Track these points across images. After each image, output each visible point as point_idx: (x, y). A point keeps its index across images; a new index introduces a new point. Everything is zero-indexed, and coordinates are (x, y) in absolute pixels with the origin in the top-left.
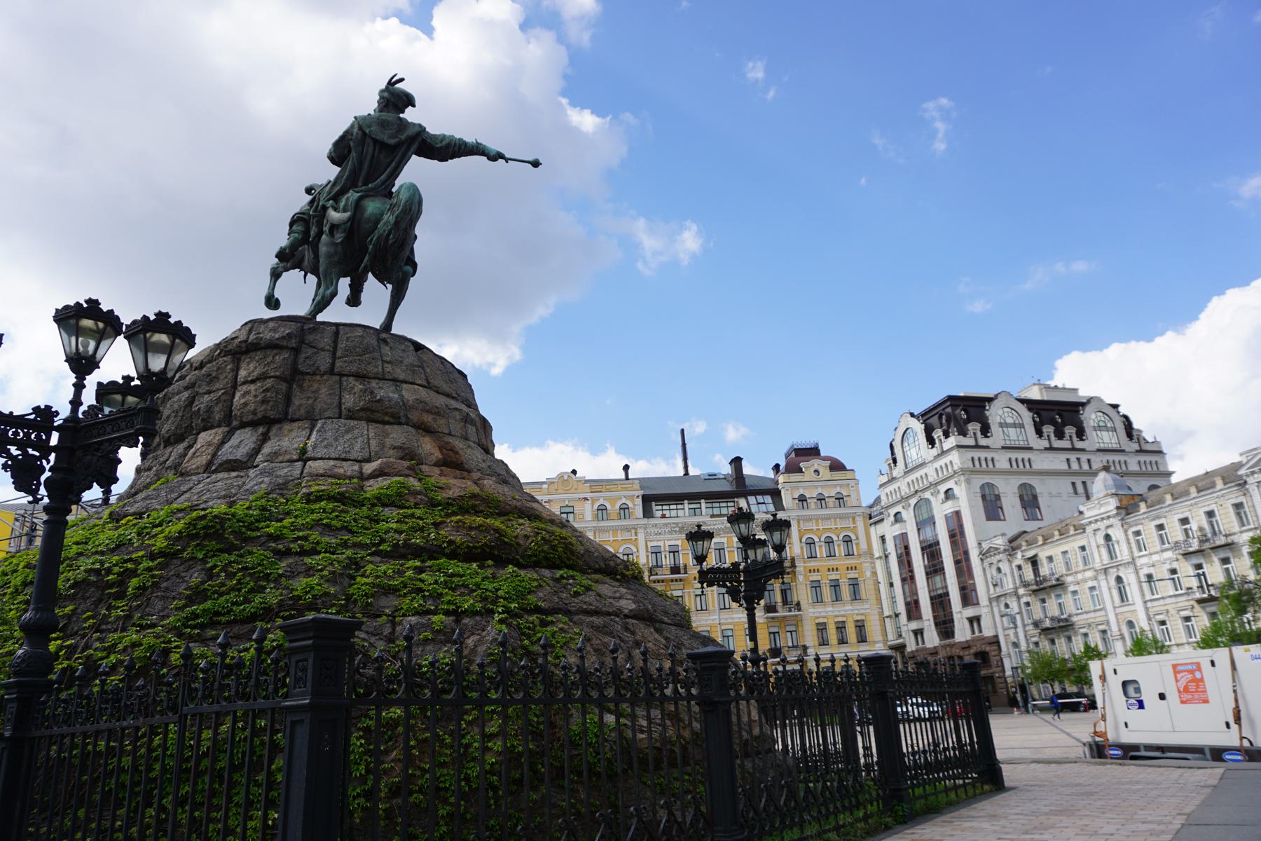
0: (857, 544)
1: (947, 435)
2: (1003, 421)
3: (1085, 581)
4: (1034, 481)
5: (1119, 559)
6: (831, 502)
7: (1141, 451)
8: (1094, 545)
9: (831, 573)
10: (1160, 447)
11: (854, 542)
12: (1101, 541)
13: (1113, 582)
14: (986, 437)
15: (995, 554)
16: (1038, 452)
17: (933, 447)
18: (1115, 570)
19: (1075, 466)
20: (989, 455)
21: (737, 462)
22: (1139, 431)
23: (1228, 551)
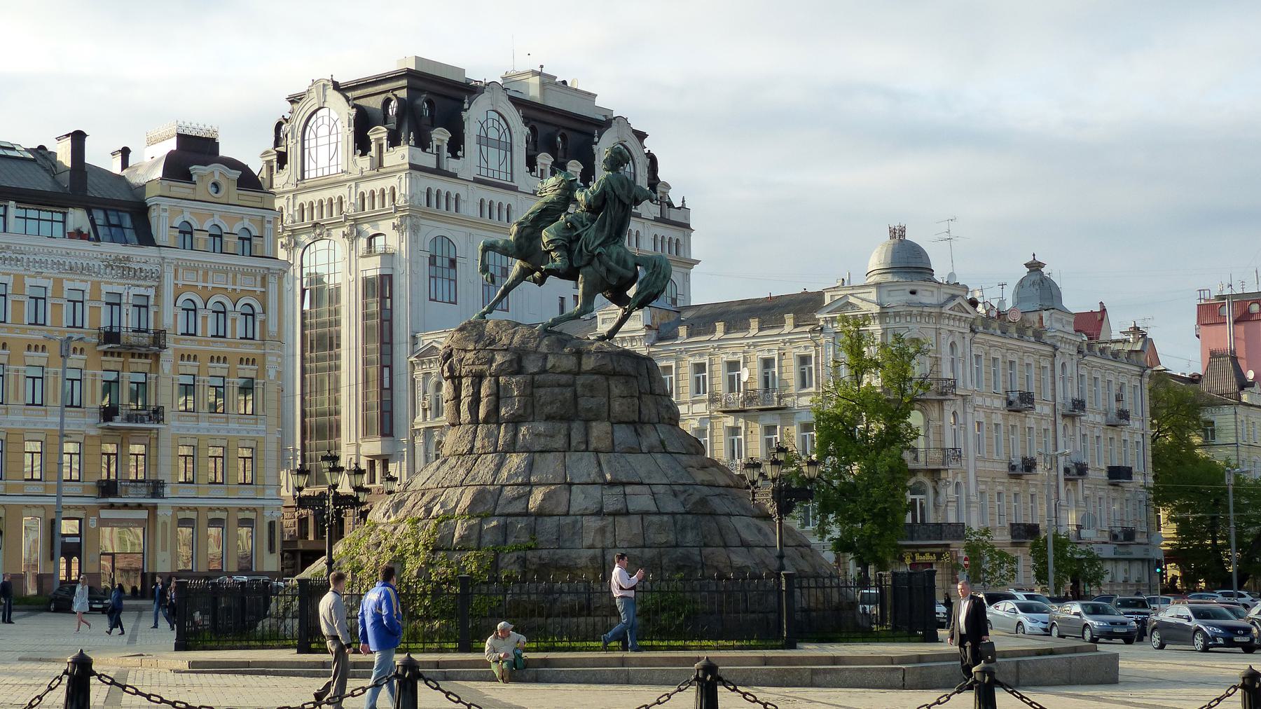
0: (263, 323)
1: (394, 140)
2: (483, 134)
6: (231, 243)
7: (662, 220)
9: (215, 364)
10: (687, 218)
11: (259, 318)
14: (455, 156)
17: (363, 154)
21: (78, 138)
22: (667, 186)
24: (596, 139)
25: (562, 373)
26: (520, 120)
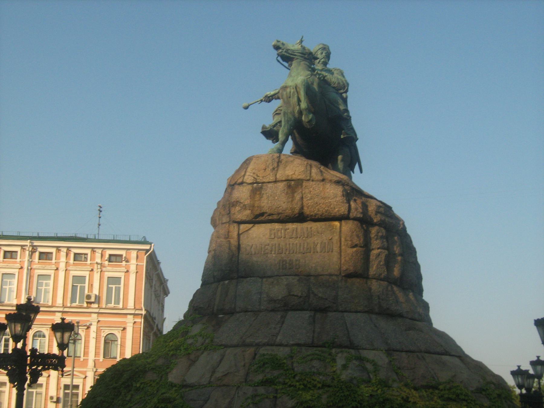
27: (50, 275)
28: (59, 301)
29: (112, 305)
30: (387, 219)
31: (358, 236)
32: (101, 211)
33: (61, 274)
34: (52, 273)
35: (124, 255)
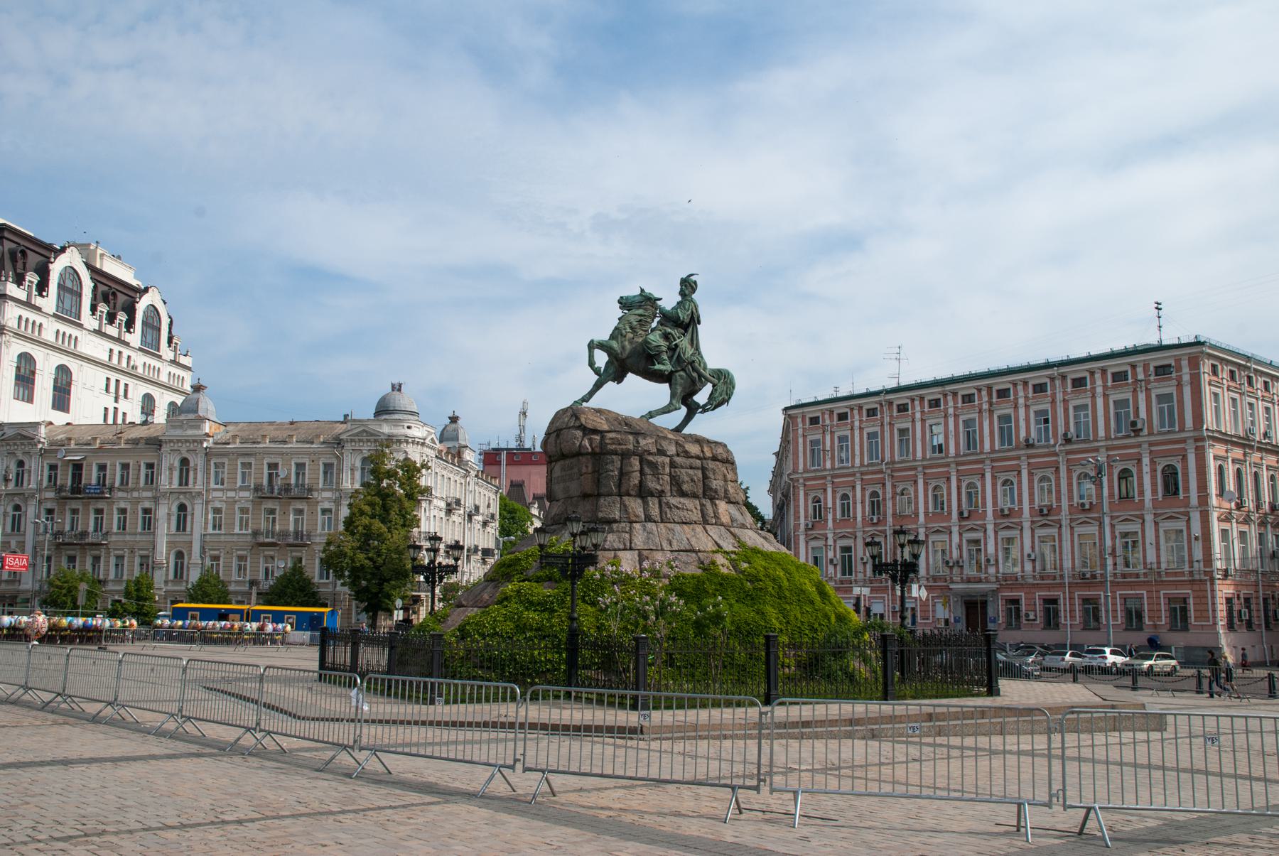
2: (62, 283)
3: (138, 500)
4: (73, 364)
5: (190, 486)
7: (174, 362)
8: (165, 465)
12: (177, 464)
13: (174, 509)
14: (41, 295)
15: (22, 444)
16: (87, 332)
18: (181, 497)
19: (115, 360)
20: (39, 319)
23: (305, 504)
24: (138, 300)
25: (692, 457)
26: (89, 277)
27: (1087, 405)
28: (1101, 433)
29: (1167, 429)
30: (618, 447)
31: (587, 467)
32: (1160, 309)
33: (1100, 401)
34: (1088, 401)
35: (1173, 364)
